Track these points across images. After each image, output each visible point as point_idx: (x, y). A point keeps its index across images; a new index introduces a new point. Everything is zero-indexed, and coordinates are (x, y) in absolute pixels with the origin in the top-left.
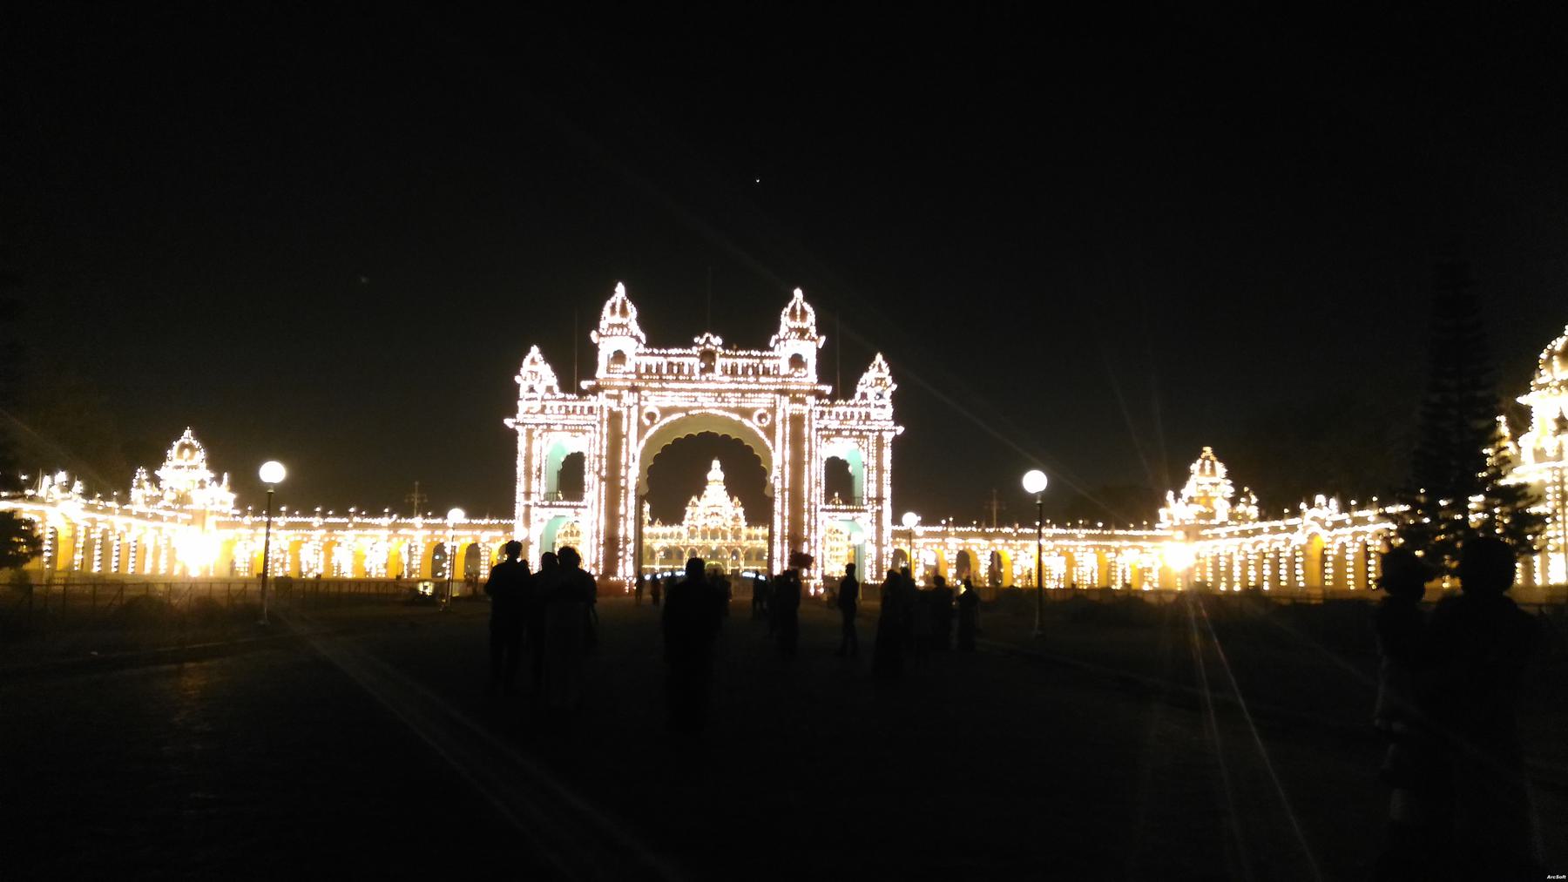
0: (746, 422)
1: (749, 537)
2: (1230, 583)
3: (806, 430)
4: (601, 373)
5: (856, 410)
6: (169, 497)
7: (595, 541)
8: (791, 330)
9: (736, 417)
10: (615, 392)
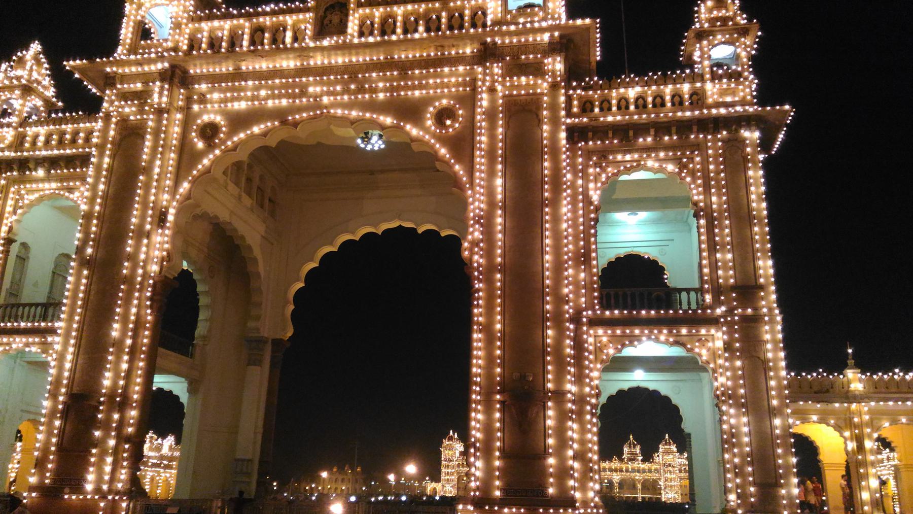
10: (139, 86)
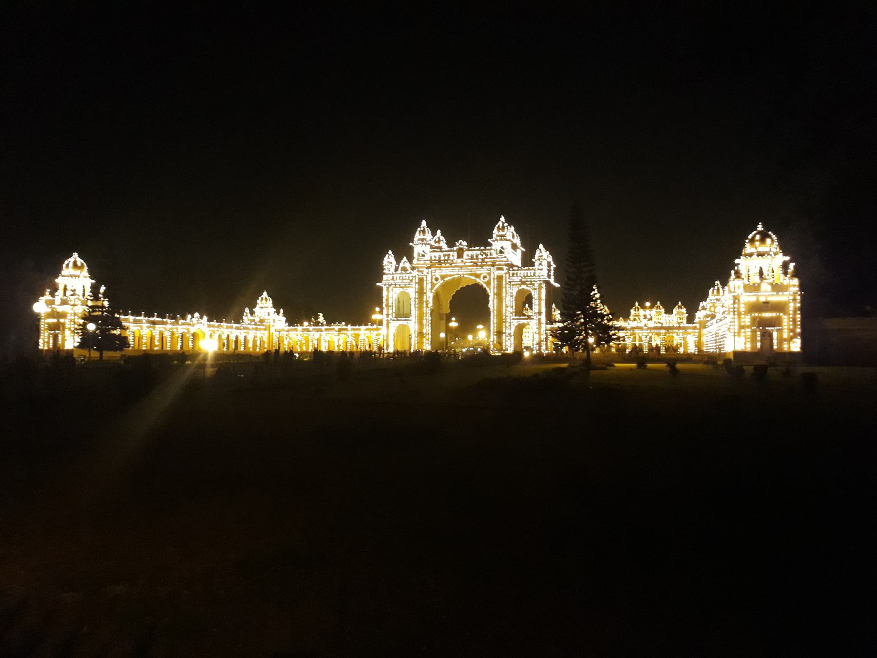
0: (478, 280)
2: (307, 347)
3: (504, 283)
6: (257, 319)
8: (498, 236)
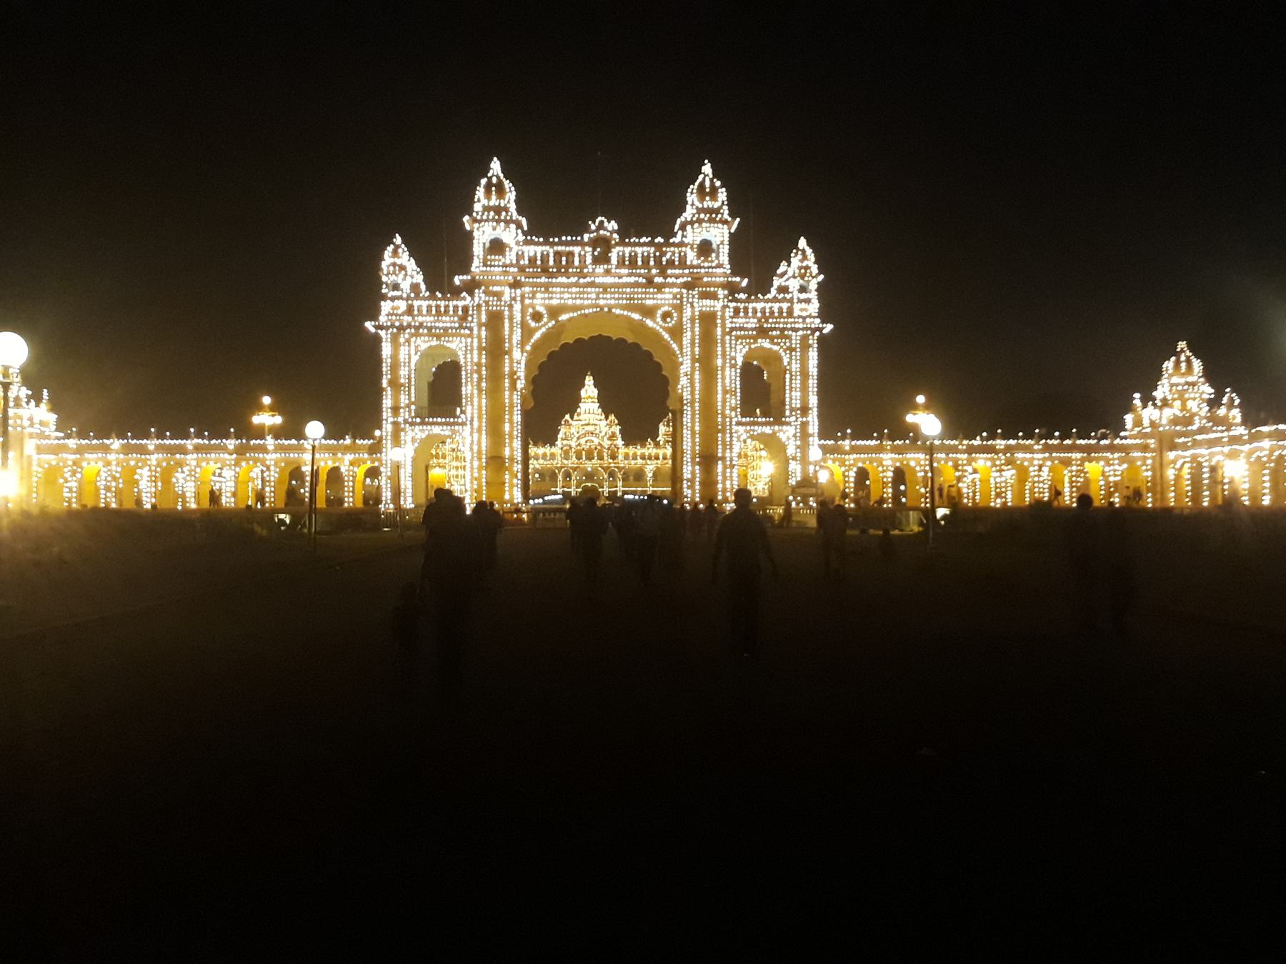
0: (649, 323)
1: (626, 457)
3: (719, 331)
4: (476, 266)
5: (776, 306)
7: (476, 464)
8: (700, 211)
9: (636, 316)
